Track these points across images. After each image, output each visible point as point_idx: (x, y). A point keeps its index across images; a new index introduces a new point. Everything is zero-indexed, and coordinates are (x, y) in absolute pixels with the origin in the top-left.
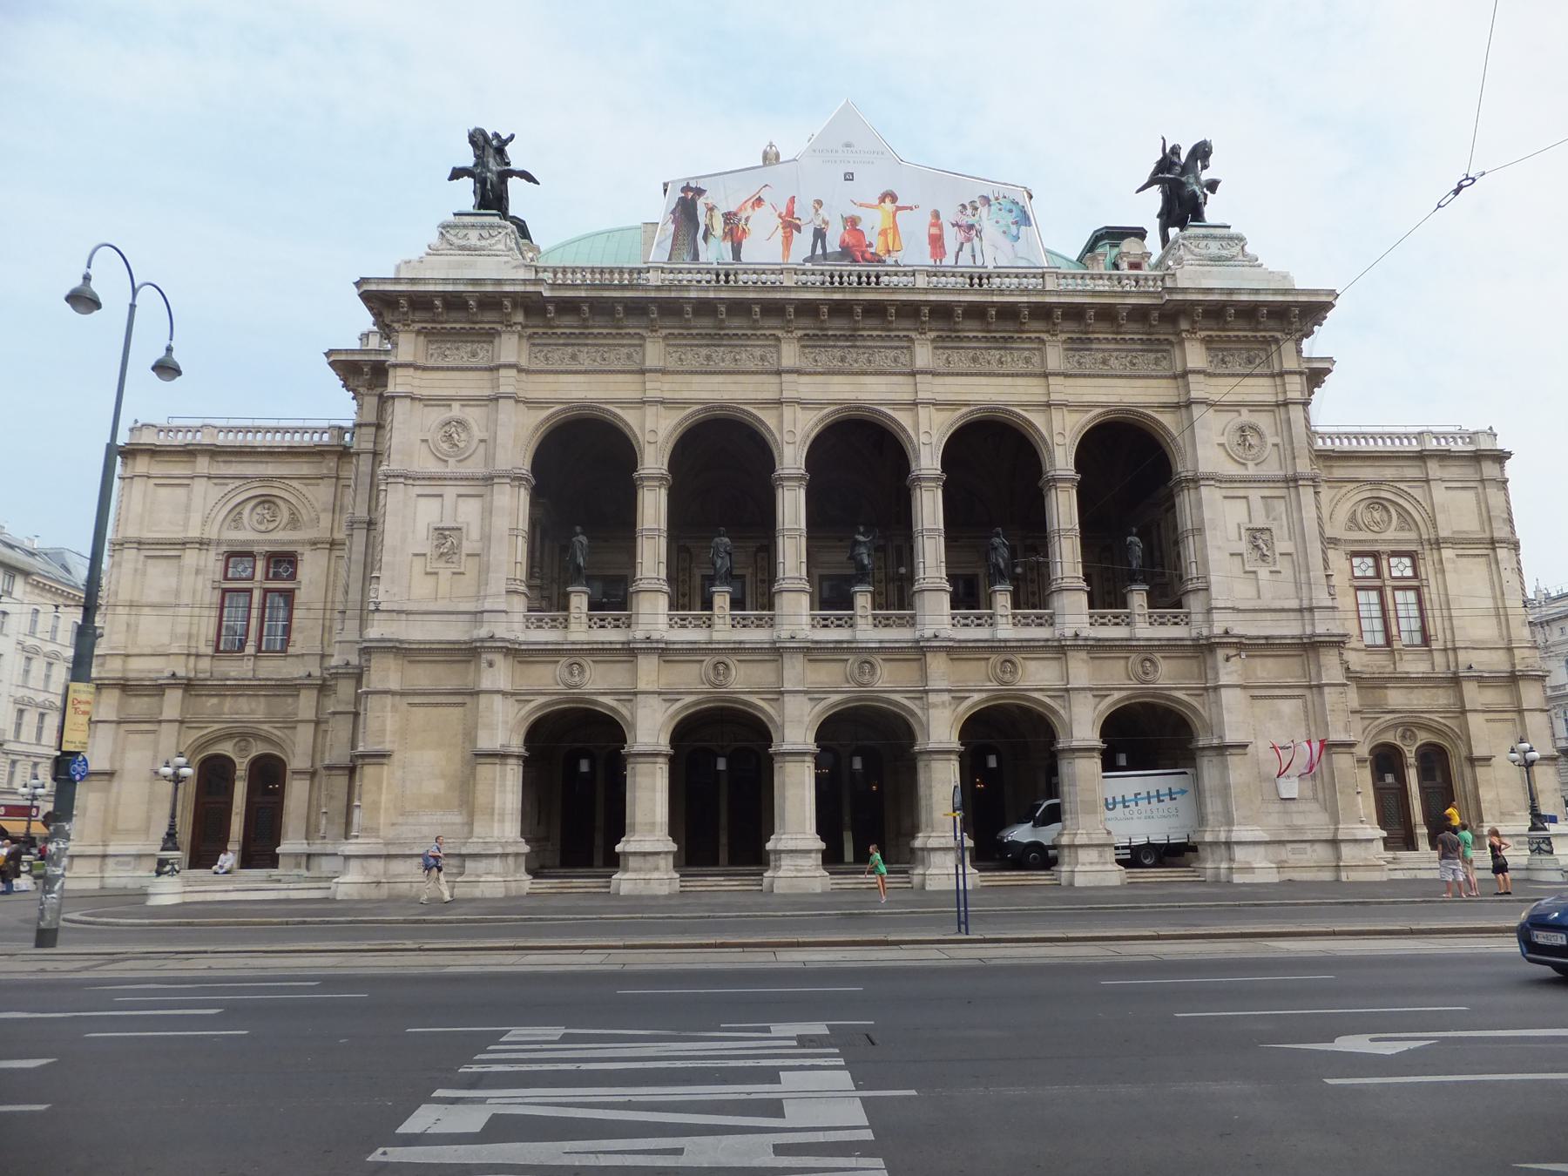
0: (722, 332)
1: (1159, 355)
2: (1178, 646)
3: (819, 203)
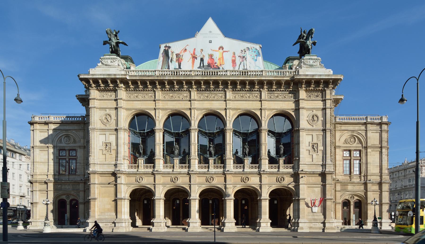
3: (202, 50)
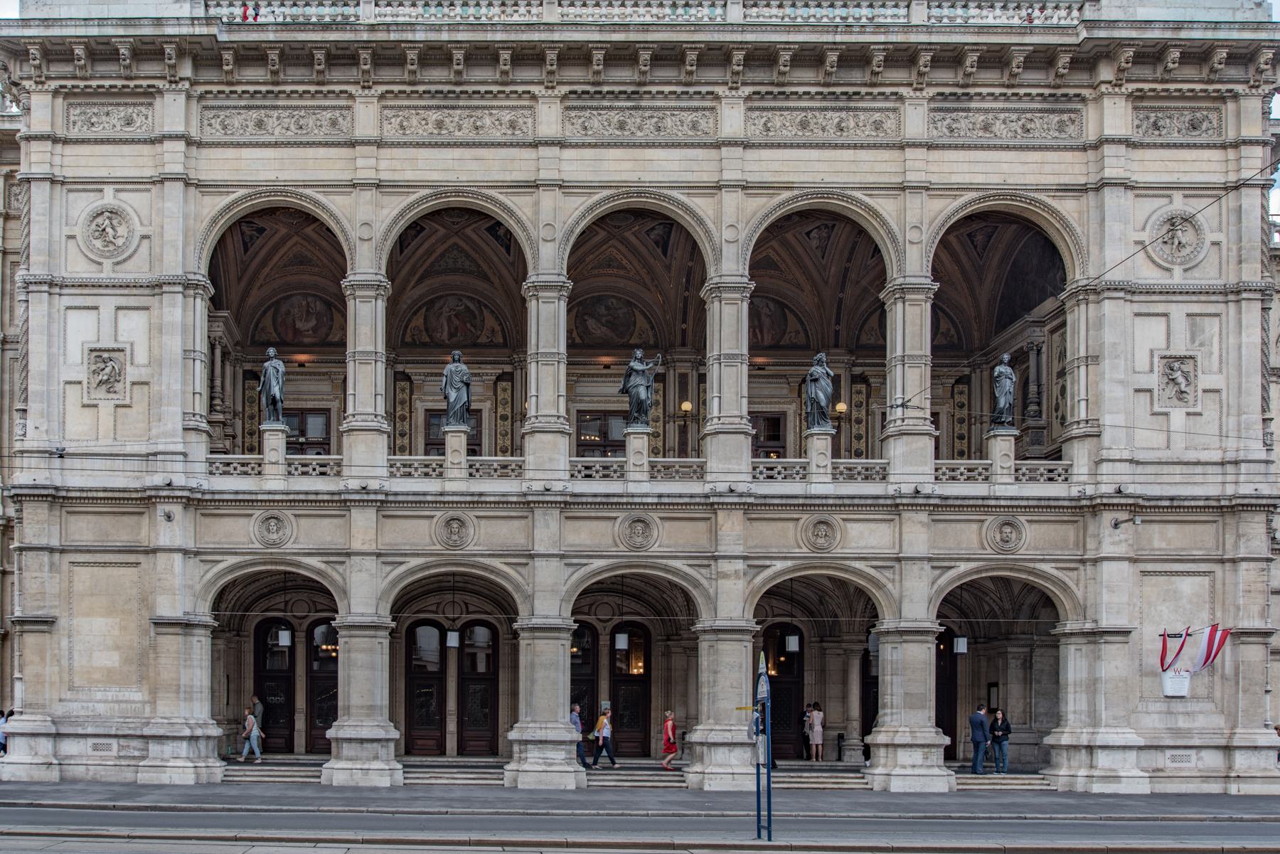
0: (458, 89)
1: (1065, 117)
2: (1050, 507)
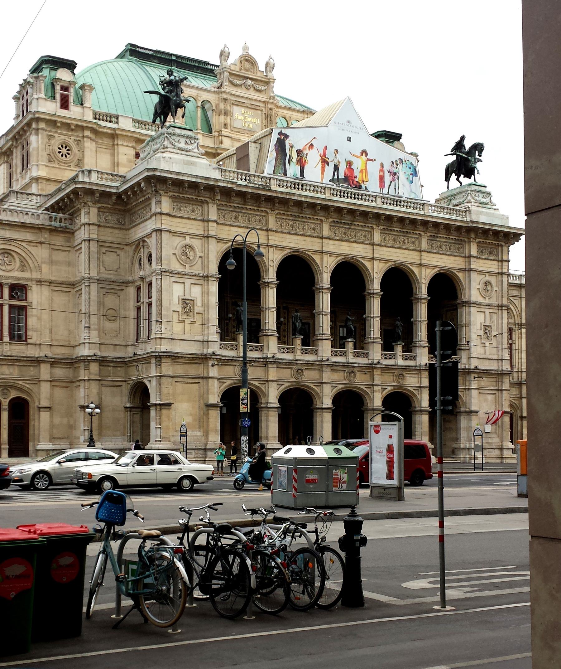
3: (337, 151)
